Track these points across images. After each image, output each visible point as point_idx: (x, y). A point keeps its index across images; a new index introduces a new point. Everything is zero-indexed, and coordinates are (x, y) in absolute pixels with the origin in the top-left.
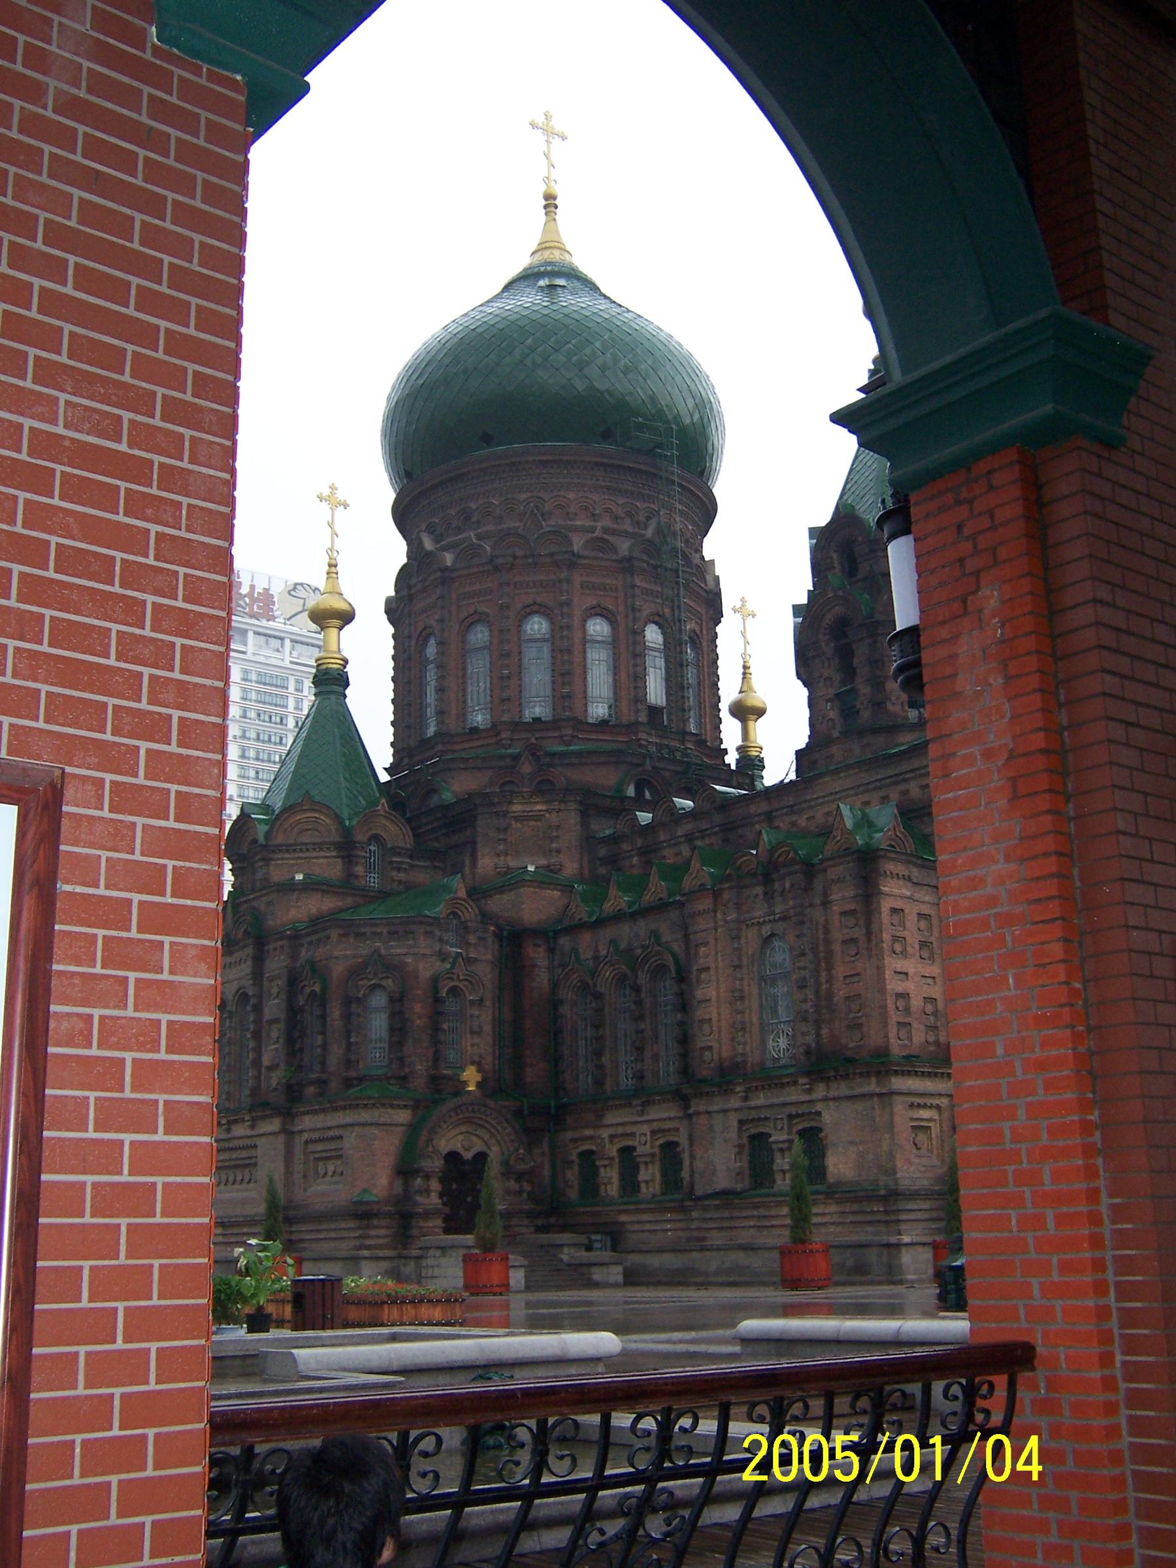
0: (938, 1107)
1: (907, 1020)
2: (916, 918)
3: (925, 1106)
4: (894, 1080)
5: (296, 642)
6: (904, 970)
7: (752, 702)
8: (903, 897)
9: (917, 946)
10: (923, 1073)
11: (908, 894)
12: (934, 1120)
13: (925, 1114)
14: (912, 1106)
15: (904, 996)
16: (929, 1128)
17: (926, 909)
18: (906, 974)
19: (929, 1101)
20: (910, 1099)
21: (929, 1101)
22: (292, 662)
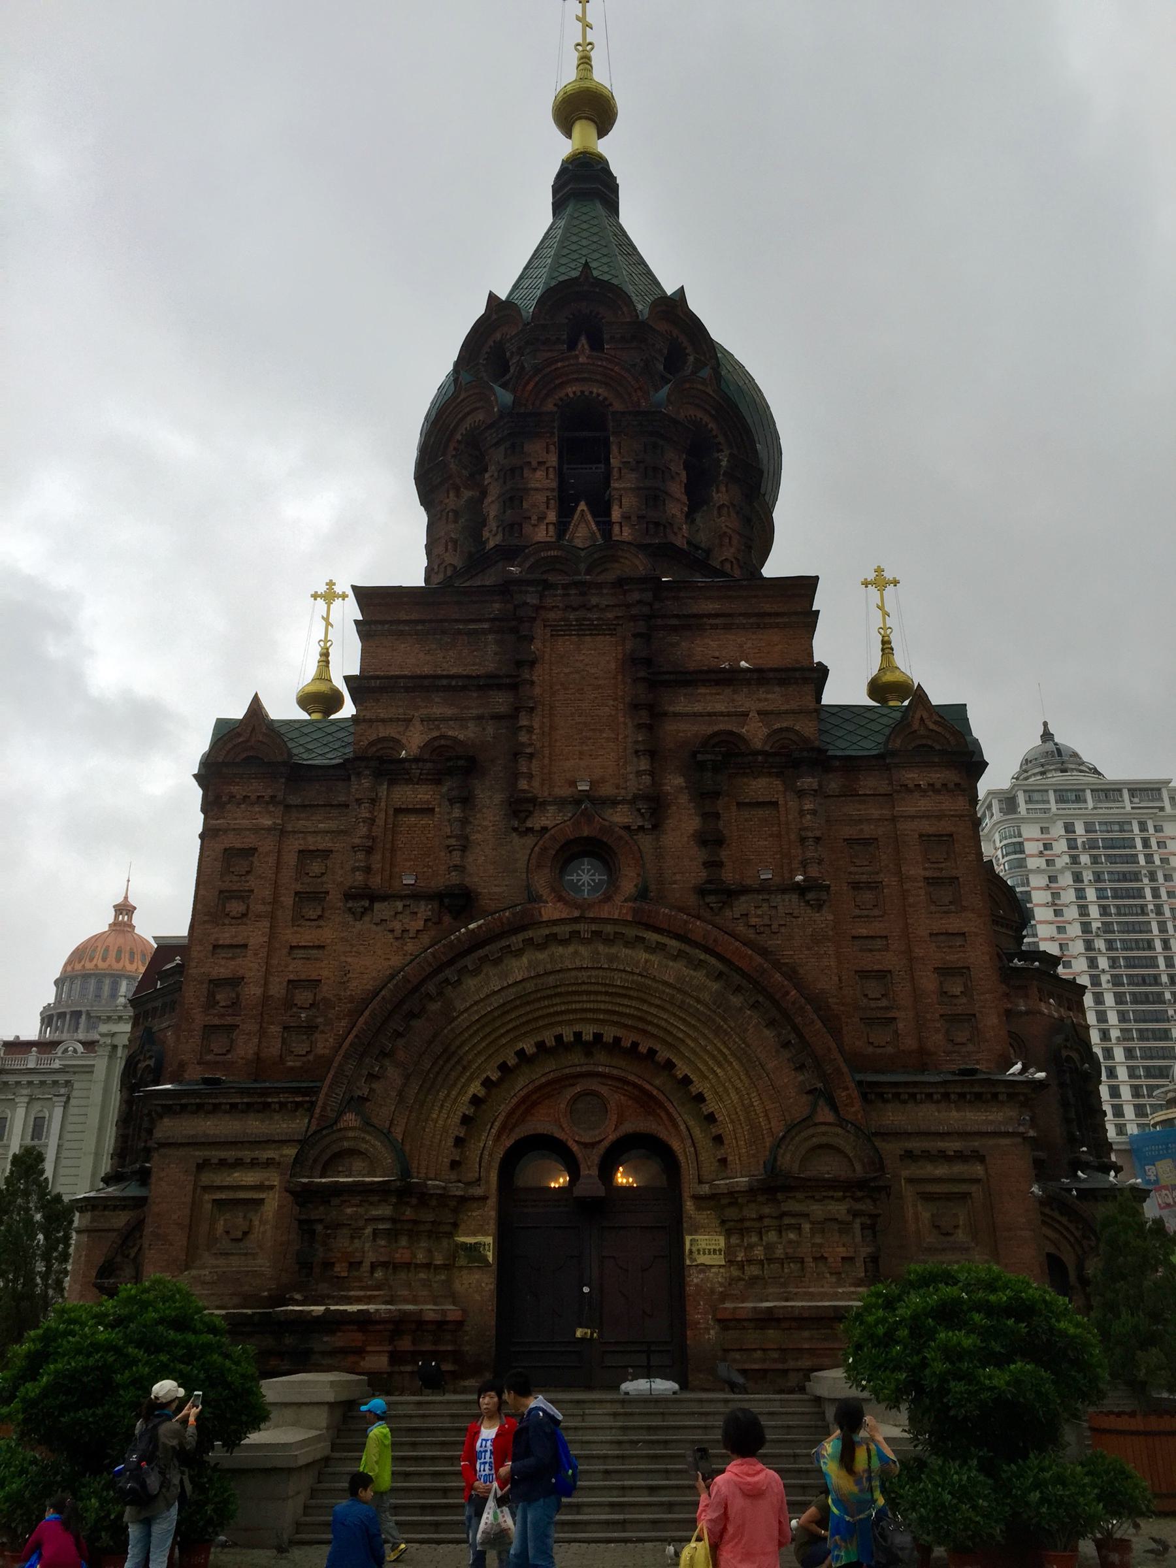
0: (269, 1163)
1: (229, 1020)
2: (291, 859)
3: (238, 1164)
4: (166, 1122)
5: (1135, 790)
6: (239, 940)
7: (889, 677)
8: (257, 830)
9: (288, 900)
10: (234, 1106)
11: (268, 822)
12: (272, 1187)
13: (250, 1178)
14: (202, 1166)
15: (235, 982)
16: (261, 1201)
17: (324, 843)
18: (245, 946)
19: (247, 1155)
20: (200, 1154)
21: (247, 1155)
22: (1132, 808)
